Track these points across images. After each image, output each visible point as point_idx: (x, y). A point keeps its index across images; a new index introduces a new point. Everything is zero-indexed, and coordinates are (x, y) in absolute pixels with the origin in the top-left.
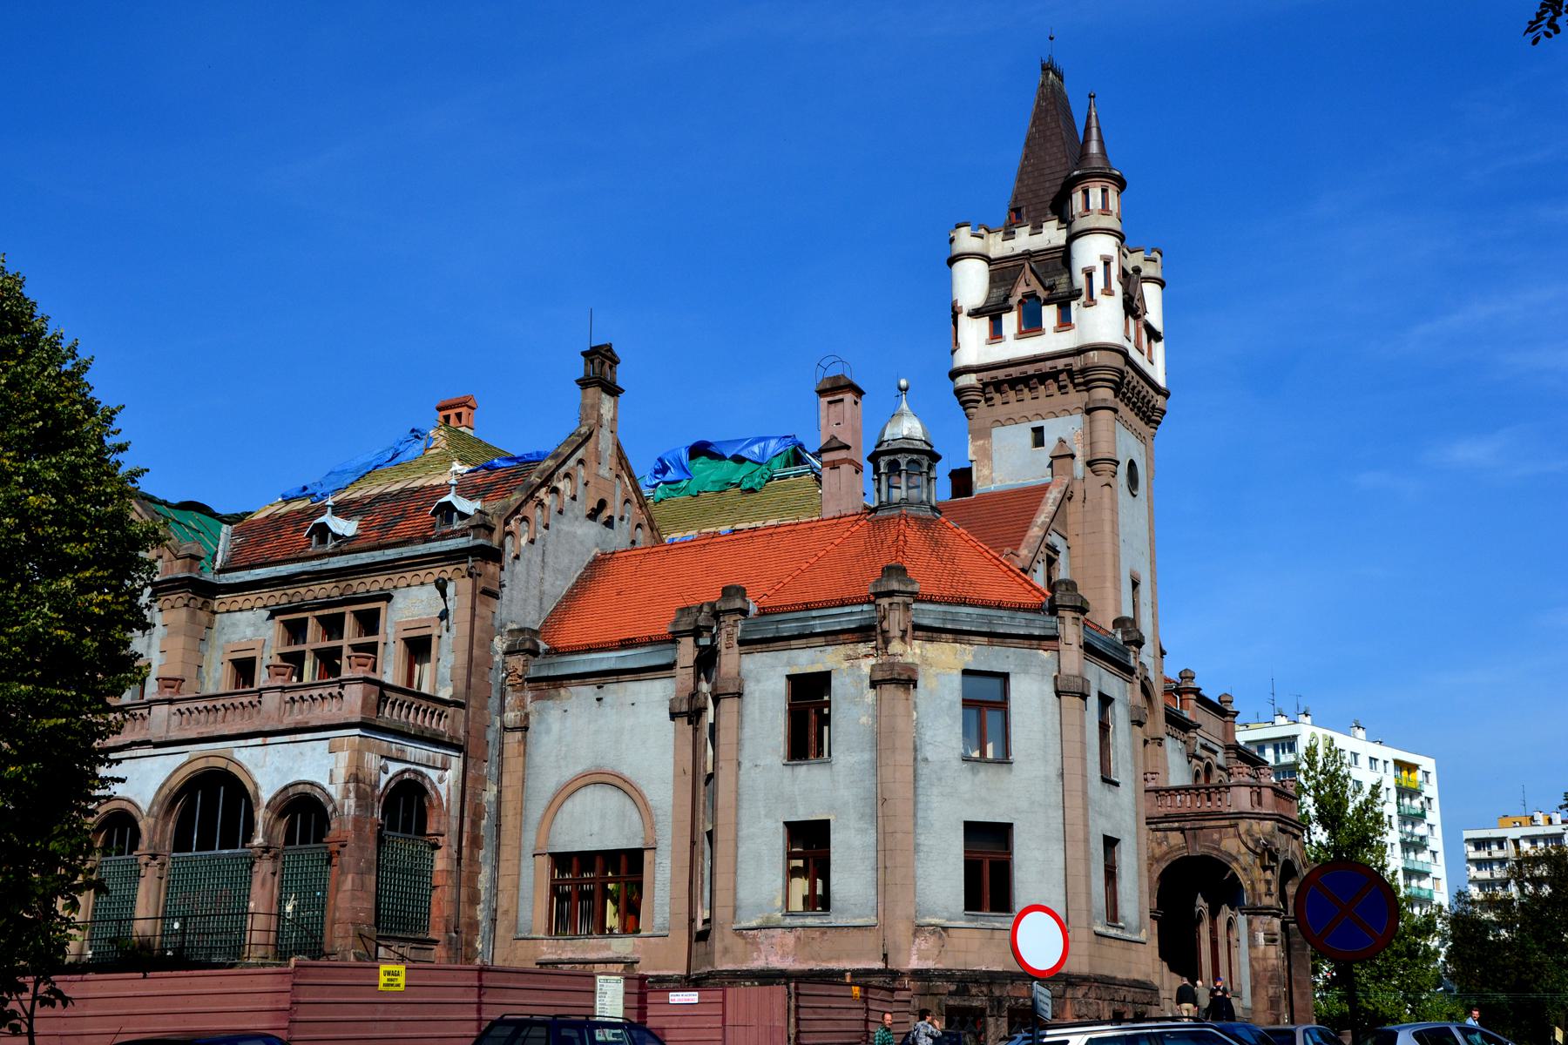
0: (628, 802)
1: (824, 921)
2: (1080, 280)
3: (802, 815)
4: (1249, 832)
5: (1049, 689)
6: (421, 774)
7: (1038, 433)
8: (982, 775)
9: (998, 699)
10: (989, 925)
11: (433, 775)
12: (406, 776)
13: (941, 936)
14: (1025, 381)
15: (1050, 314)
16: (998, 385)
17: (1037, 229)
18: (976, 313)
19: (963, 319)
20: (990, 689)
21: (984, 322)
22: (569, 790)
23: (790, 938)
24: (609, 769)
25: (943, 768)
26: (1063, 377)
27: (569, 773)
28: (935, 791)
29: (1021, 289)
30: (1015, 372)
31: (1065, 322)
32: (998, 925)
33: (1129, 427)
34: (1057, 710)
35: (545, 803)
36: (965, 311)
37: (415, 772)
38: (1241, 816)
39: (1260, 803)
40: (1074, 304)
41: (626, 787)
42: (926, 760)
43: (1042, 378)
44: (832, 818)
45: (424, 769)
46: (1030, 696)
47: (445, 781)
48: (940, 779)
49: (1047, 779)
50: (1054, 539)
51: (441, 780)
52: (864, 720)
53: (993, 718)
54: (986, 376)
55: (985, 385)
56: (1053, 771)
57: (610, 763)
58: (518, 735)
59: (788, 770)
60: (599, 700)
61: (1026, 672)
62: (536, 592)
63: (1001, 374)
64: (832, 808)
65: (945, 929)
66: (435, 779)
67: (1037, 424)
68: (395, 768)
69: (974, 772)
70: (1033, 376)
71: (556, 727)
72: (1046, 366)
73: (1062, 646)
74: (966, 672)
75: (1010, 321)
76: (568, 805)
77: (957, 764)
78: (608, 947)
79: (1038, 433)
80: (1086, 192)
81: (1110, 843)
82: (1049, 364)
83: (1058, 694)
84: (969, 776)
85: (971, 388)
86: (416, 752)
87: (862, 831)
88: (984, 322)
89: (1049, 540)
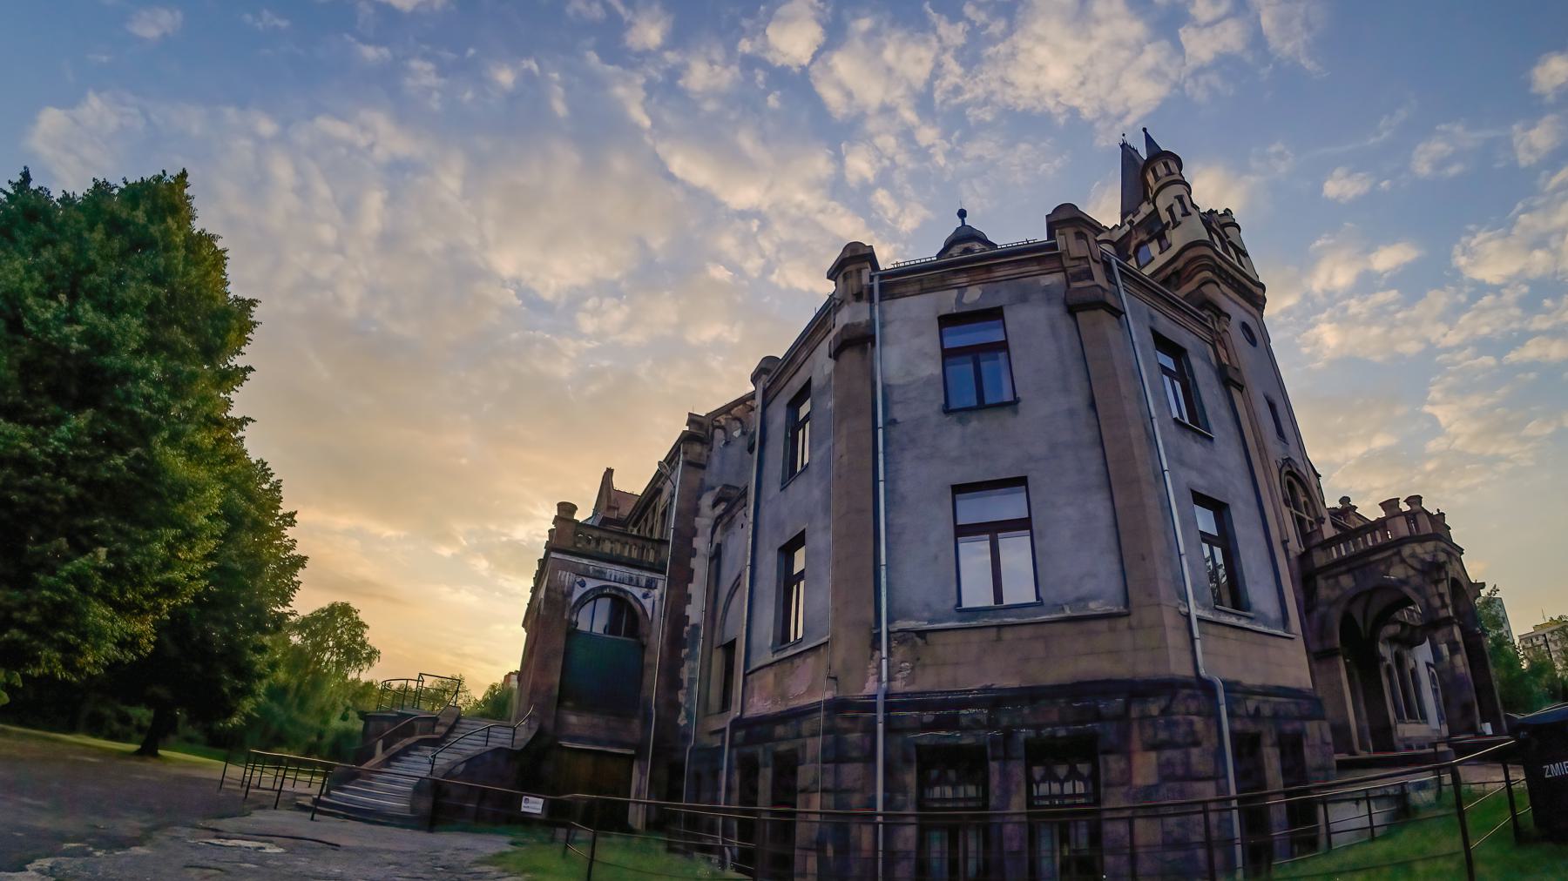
10: (995, 622)
11: (638, 592)
13: (914, 645)
42: (890, 423)
45: (627, 588)
47: (652, 600)
49: (1072, 413)
51: (645, 596)
56: (1079, 400)
65: (922, 634)
84: (957, 430)
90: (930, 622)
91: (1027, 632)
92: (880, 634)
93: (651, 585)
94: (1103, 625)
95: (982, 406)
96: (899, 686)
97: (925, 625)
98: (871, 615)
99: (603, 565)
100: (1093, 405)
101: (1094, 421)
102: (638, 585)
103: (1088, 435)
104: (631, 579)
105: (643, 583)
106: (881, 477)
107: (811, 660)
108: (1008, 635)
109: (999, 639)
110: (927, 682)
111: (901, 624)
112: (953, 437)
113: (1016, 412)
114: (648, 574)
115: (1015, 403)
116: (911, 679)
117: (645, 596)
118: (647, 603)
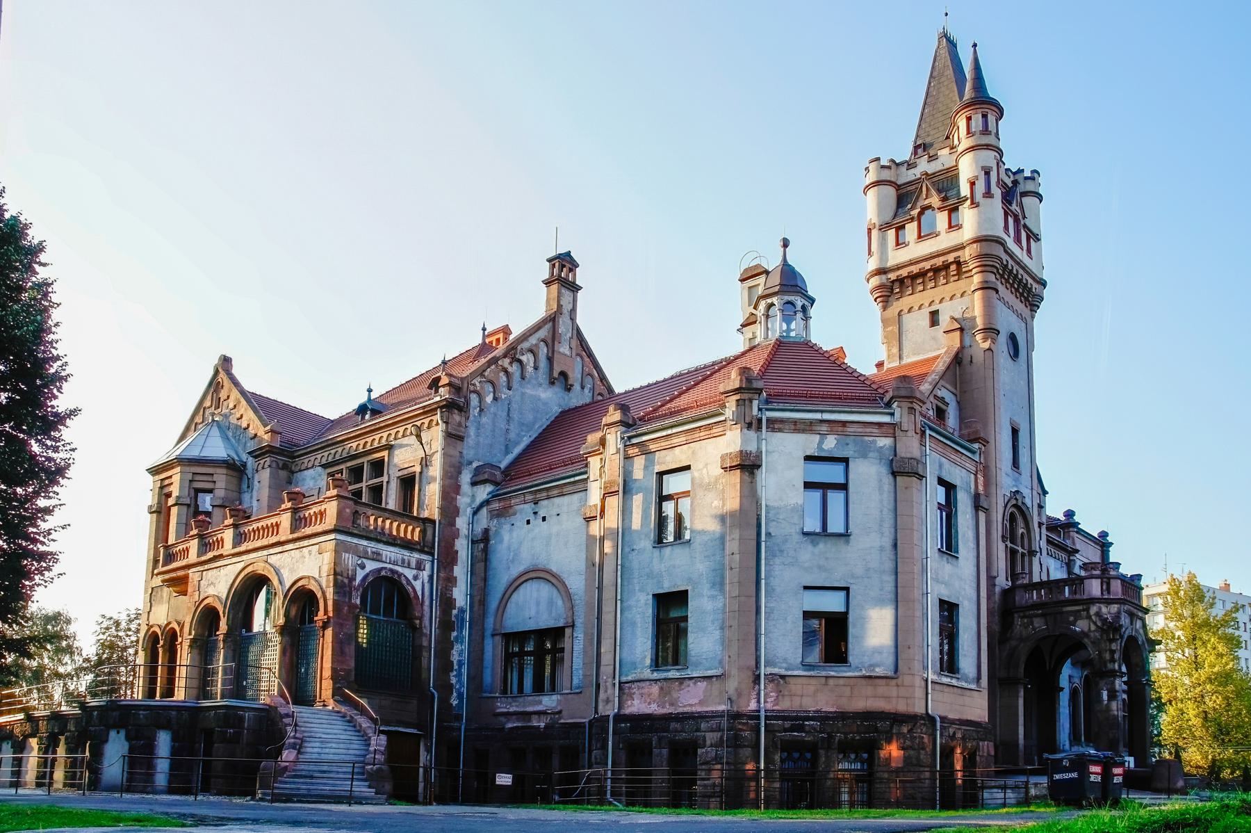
0: (555, 592)
2: (965, 190)
3: (667, 587)
4: (1098, 614)
5: (884, 471)
6: (397, 572)
7: (934, 316)
8: (821, 546)
9: (842, 481)
10: (824, 673)
11: (409, 573)
12: (383, 573)
14: (922, 274)
15: (942, 219)
16: (901, 281)
19: (875, 233)
20: (833, 473)
21: (891, 233)
22: (515, 585)
23: (655, 689)
24: (541, 567)
25: (786, 541)
26: (953, 267)
27: (516, 571)
28: (777, 560)
30: (915, 269)
32: (832, 673)
33: (1006, 303)
34: (892, 488)
35: (499, 595)
37: (391, 570)
38: (1093, 601)
39: (1109, 593)
42: (768, 534)
43: (936, 270)
44: (689, 588)
46: (868, 475)
47: (419, 578)
48: (781, 551)
49: (882, 549)
50: (949, 397)
51: (416, 578)
52: (716, 503)
53: (835, 498)
55: (893, 282)
56: (887, 542)
57: (542, 562)
58: (482, 545)
59: (656, 552)
60: (535, 513)
61: (864, 456)
62: (502, 439)
63: (904, 272)
64: (689, 580)
65: (783, 677)
66: (410, 577)
67: (933, 308)
68: (371, 566)
69: (814, 544)
70: (928, 271)
71: (506, 538)
72: (939, 262)
73: (898, 432)
74: (808, 458)
75: (911, 230)
76: (515, 596)
77: (797, 537)
79: (934, 316)
81: (949, 610)
82: (942, 259)
83: (894, 474)
84: (810, 547)
86: (389, 552)
87: (713, 597)
89: (939, 394)
90: (787, 669)
91: (841, 681)
92: (758, 676)
93: (419, 566)
94: (883, 682)
95: (824, 533)
96: (769, 706)
97: (783, 672)
98: (754, 663)
99: (380, 546)
100: (895, 546)
101: (893, 557)
102: (409, 567)
103: (889, 565)
104: (403, 560)
105: (413, 564)
106: (763, 576)
107: (702, 685)
108: (831, 682)
109: (826, 684)
110: (785, 705)
111: (770, 670)
112: (807, 553)
113: (848, 542)
114: (416, 555)
115: (845, 536)
116: (776, 702)
117: (416, 578)
118: (418, 585)
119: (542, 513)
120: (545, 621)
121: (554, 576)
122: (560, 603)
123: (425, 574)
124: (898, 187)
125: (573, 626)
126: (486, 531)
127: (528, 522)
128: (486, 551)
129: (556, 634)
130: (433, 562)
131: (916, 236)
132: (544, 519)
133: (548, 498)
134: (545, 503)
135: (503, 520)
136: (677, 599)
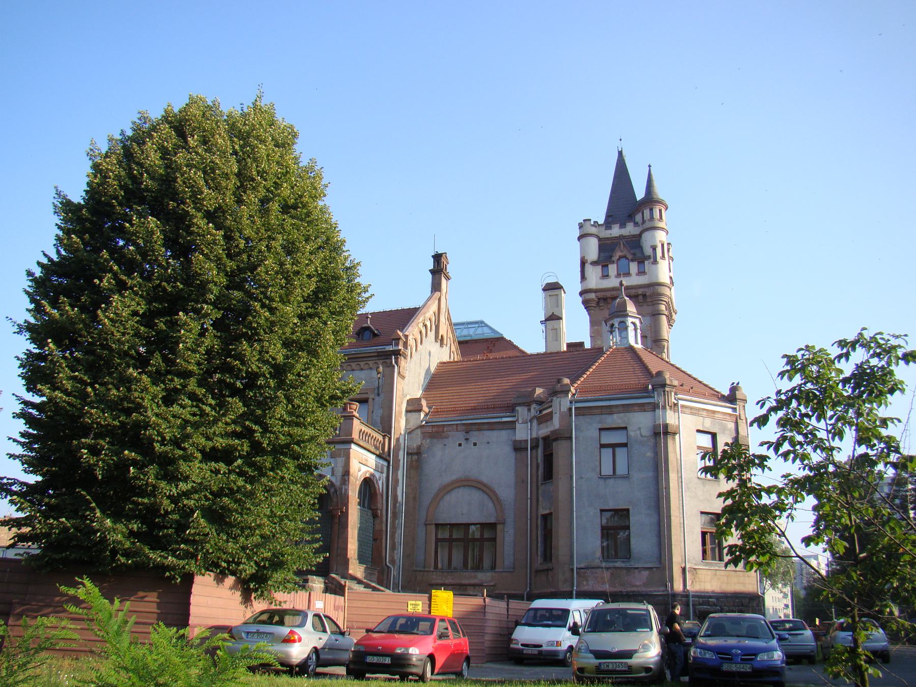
0: (486, 497)
1: (628, 565)
15: (634, 267)
17: (623, 225)
18: (594, 263)
21: (599, 268)
27: (448, 479)
29: (618, 254)
31: (641, 273)
36: (589, 262)
40: (646, 262)
41: (485, 489)
54: (600, 295)
58: (415, 457)
75: (612, 269)
76: (447, 498)
78: (475, 577)
80: (651, 210)
85: (592, 300)
88: (599, 268)
119: (473, 440)
120: (477, 517)
121: (485, 485)
122: (490, 505)
123: (385, 475)
124: (600, 239)
125: (504, 523)
126: (419, 447)
127: (460, 445)
128: (418, 461)
129: (492, 526)
130: (388, 467)
131: (616, 273)
132: (475, 444)
133: (479, 430)
134: (476, 433)
135: (435, 441)
136: (624, 513)
